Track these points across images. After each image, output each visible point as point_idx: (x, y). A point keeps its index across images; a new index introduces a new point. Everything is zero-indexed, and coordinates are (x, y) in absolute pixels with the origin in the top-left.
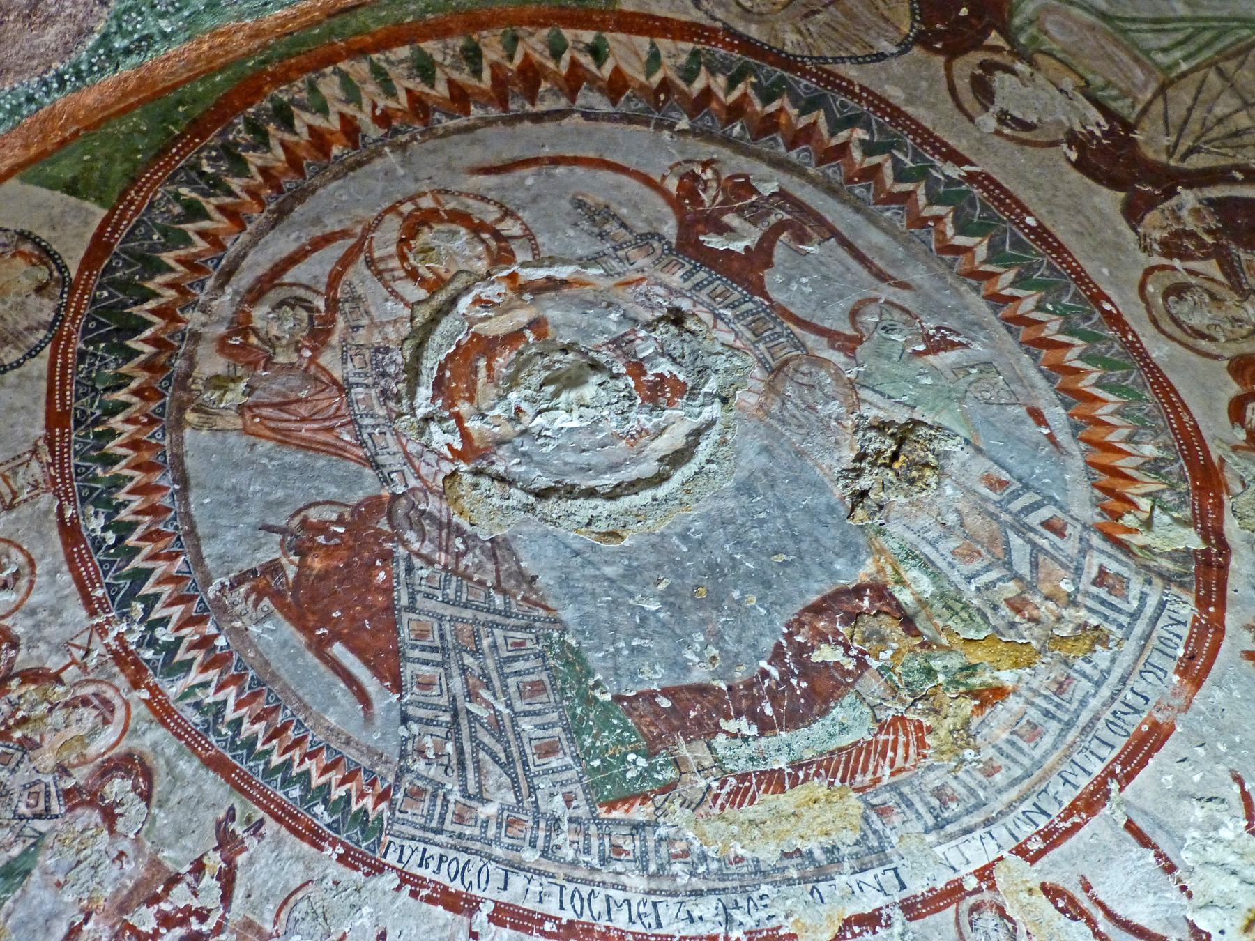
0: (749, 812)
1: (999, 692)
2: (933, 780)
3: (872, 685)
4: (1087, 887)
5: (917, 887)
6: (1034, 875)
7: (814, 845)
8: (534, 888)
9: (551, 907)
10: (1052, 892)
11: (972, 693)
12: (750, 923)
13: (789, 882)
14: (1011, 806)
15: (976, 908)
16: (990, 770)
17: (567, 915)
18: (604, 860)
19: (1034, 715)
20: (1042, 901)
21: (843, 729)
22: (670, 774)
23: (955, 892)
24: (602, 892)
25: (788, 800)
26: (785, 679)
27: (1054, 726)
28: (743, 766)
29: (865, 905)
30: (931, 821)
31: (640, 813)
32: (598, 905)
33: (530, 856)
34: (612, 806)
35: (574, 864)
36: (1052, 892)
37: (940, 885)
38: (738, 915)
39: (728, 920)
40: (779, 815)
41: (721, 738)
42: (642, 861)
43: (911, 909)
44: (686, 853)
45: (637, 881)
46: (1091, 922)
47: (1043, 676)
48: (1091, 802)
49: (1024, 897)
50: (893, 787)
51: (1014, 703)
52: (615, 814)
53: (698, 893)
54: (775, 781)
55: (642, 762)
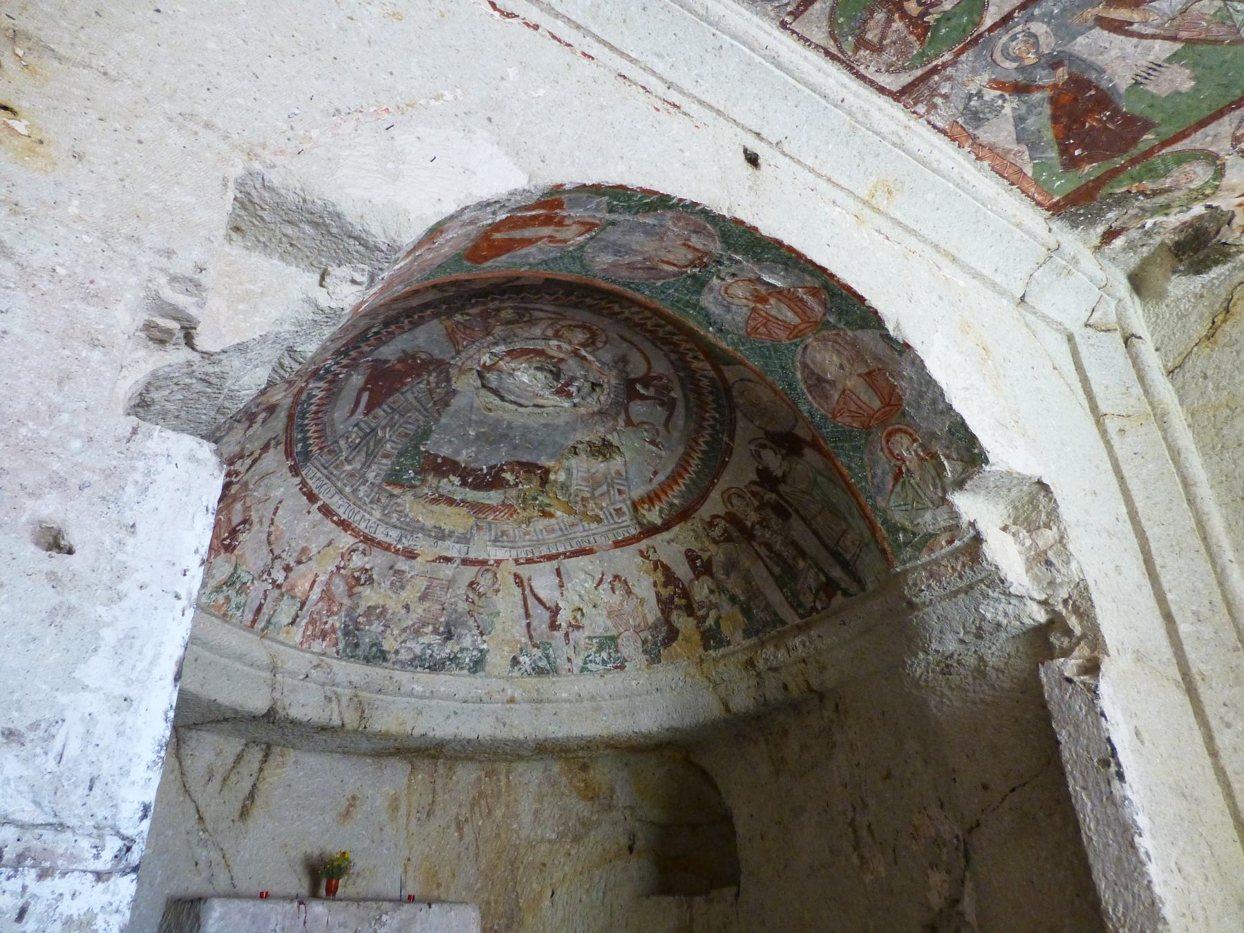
0: (435, 508)
1: (551, 515)
2: (505, 527)
3: (513, 492)
4: (530, 579)
5: (472, 556)
7: (447, 528)
10: (516, 576)
11: (543, 512)
12: (407, 544)
13: (430, 536)
14: (524, 546)
15: (487, 570)
16: (527, 533)
19: (556, 527)
20: (511, 578)
21: (489, 498)
22: (418, 483)
23: (484, 563)
25: (449, 510)
26: (486, 475)
27: (560, 533)
28: (444, 492)
29: (449, 554)
30: (493, 538)
36: (516, 576)
37: (480, 558)
38: (404, 540)
39: (400, 540)
40: (443, 513)
41: (445, 480)
42: (384, 508)
44: (401, 512)
46: (524, 590)
47: (568, 519)
48: (550, 558)
49: (506, 574)
50: (490, 524)
51: (553, 521)
53: (395, 527)
54: (451, 502)
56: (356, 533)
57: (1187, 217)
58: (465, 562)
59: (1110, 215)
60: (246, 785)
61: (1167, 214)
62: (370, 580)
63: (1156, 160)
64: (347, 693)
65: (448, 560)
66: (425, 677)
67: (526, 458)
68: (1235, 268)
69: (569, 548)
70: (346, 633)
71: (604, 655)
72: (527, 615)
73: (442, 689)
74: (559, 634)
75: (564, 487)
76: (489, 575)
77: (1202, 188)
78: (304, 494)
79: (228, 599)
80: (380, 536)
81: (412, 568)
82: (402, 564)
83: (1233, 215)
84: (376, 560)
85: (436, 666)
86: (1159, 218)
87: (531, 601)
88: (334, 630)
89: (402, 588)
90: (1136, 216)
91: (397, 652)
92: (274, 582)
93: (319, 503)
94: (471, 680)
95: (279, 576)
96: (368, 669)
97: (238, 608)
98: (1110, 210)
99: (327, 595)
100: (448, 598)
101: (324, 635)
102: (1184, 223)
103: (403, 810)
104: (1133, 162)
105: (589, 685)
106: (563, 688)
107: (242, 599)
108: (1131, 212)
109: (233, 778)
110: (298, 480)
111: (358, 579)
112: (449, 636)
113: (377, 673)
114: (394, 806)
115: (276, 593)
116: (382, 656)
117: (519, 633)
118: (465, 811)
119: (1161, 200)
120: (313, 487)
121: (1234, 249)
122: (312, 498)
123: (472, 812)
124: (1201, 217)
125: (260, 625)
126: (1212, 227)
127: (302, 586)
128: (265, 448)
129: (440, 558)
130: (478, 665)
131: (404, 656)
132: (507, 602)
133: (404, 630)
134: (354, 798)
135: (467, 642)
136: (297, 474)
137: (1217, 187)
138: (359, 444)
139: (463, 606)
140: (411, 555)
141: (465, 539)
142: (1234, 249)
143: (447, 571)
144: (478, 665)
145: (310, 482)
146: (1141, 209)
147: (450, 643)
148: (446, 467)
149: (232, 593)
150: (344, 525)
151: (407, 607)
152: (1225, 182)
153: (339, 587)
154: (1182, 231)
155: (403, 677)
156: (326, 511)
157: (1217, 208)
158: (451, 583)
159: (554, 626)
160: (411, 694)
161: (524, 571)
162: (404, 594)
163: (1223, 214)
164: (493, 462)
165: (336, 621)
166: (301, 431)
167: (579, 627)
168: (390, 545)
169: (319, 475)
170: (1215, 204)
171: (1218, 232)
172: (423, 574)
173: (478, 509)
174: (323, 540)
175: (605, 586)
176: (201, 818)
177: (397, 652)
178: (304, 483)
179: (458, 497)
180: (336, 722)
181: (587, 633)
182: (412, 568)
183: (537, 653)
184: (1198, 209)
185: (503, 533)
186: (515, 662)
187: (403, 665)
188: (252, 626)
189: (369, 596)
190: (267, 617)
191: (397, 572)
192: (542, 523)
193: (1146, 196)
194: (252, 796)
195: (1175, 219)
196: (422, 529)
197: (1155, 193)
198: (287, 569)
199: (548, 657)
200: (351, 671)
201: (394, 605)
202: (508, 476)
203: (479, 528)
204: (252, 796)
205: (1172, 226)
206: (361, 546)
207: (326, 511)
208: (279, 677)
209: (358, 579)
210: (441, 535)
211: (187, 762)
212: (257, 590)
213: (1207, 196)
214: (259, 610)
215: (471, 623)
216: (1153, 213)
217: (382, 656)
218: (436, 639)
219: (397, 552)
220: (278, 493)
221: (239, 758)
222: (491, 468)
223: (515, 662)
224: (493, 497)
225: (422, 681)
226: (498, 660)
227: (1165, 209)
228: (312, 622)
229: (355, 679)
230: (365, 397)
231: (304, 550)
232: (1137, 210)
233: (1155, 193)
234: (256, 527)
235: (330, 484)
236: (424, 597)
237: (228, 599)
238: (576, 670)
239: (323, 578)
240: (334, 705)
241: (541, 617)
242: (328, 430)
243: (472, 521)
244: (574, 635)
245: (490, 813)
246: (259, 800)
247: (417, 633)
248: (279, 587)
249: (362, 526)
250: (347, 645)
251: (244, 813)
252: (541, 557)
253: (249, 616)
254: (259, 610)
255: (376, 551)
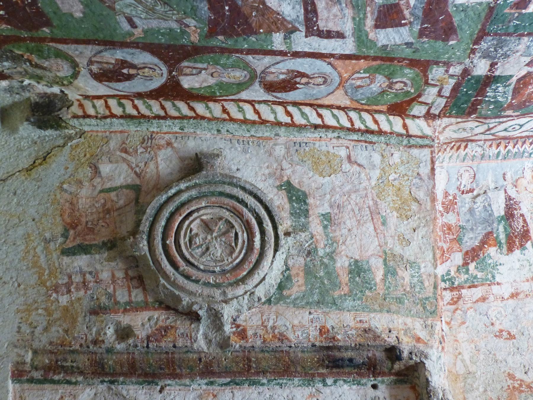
57: (49, 90)
59: (5, 64)
61: (38, 83)
63: (45, 46)
68: (60, 135)
77: (62, 78)
83: (72, 105)
86: (33, 82)
90: (20, 73)
98: (7, 60)
102: (46, 94)
104: (32, 39)
108: (19, 69)
119: (39, 72)
121: (64, 124)
124: (55, 95)
126: (59, 104)
137: (71, 83)
142: (64, 124)
146: (26, 71)
152: (76, 82)
154: (42, 97)
157: (66, 95)
163: (68, 100)
170: (66, 92)
171: (60, 109)
184: (56, 90)
193: (31, 64)
195: (41, 88)
197: (37, 66)
205: (38, 91)
213: (63, 85)
216: (32, 77)
227: (39, 79)
232: (22, 70)
233: (37, 66)
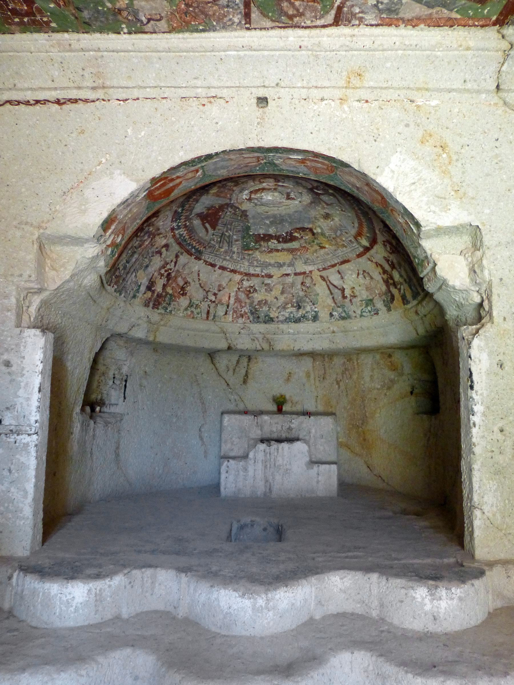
2: (307, 256)
4: (327, 277)
5: (298, 271)
6: (319, 273)
7: (281, 262)
8: (227, 263)
9: (230, 266)
14: (319, 263)
15: (307, 276)
17: (232, 268)
18: (241, 259)
20: (319, 277)
22: (258, 247)
23: (304, 273)
24: (240, 265)
25: (278, 254)
28: (273, 247)
30: (304, 262)
31: (250, 252)
32: (238, 267)
33: (228, 258)
34: (245, 250)
35: (236, 259)
37: (302, 271)
40: (276, 256)
41: (270, 243)
42: (248, 260)
43: (296, 274)
44: (257, 260)
45: (247, 263)
49: (316, 276)
50: (299, 256)
52: (246, 252)
54: (277, 251)
55: (254, 244)
56: (240, 273)
58: (296, 274)
60: (243, 371)
62: (255, 290)
64: (260, 337)
65: (288, 275)
66: (293, 325)
67: (299, 226)
69: (339, 261)
70: (252, 313)
71: (369, 308)
72: (331, 294)
73: (302, 330)
74: (347, 300)
75: (323, 234)
76: (309, 278)
78: (208, 265)
79: (192, 312)
80: (252, 271)
81: (272, 282)
82: (267, 281)
84: (255, 282)
85: (297, 321)
87: (331, 287)
88: (246, 313)
89: (271, 290)
91: (277, 317)
92: (211, 301)
93: (218, 267)
94: (314, 324)
95: (213, 298)
96: (267, 326)
97: (198, 314)
99: (238, 300)
100: (293, 291)
101: (242, 316)
103: (312, 377)
105: (365, 322)
106: (355, 324)
107: (199, 310)
109: (237, 369)
110: (202, 261)
111: (250, 291)
112: (299, 307)
113: (271, 327)
114: (308, 375)
115: (214, 304)
116: (271, 320)
117: (330, 301)
118: (340, 377)
120: (211, 261)
122: (213, 265)
123: (343, 377)
125: (211, 317)
127: (225, 299)
128: (177, 256)
129: (283, 275)
130: (315, 318)
131: (281, 318)
132: (321, 288)
133: (278, 308)
134: (290, 373)
135: (308, 308)
136: (200, 259)
138: (221, 240)
139: (302, 294)
140: (270, 276)
141: (291, 264)
143: (289, 280)
144: (315, 318)
145: (208, 260)
147: (301, 310)
148: (267, 238)
149: (192, 309)
150: (234, 271)
151: (276, 298)
153: (242, 296)
155: (284, 327)
156: (223, 268)
158: (293, 285)
159: (344, 297)
160: (289, 333)
161: (324, 273)
162: (273, 293)
164: (286, 231)
165: (246, 309)
166: (189, 246)
167: (355, 297)
168: (258, 274)
169: (211, 256)
172: (279, 283)
173: (291, 251)
174: (227, 280)
175: (361, 276)
176: (228, 385)
177: (277, 317)
178: (205, 261)
179: (280, 248)
180: (259, 348)
181: (359, 299)
182: (272, 282)
183: (340, 310)
185: (308, 259)
186: (331, 315)
187: (282, 322)
188: (207, 318)
189: (257, 297)
190: (213, 314)
191: (266, 285)
192: (322, 251)
194: (246, 375)
196: (270, 264)
198: (215, 294)
199: (345, 311)
200: (258, 328)
201: (270, 298)
202: (296, 234)
203: (296, 259)
204: (246, 375)
206: (245, 278)
207: (223, 268)
208: (228, 335)
209: (250, 291)
210: (280, 266)
211: (218, 365)
212: (204, 306)
214: (208, 312)
215: (307, 300)
217: (271, 320)
218: (294, 310)
219: (263, 276)
220: (197, 268)
221: (238, 362)
222: (287, 233)
223: (331, 315)
224: (295, 245)
225: (292, 327)
226: (324, 315)
228: (235, 312)
229: (262, 331)
230: (207, 225)
231: (220, 286)
234: (192, 283)
235: (218, 258)
236: (282, 293)
237: (192, 312)
238: (358, 316)
239: (233, 294)
240: (256, 341)
241: (337, 293)
242: (202, 241)
243: (291, 256)
244: (354, 300)
245: (351, 377)
246: (250, 376)
247: (285, 308)
248: (214, 302)
249: (242, 270)
250: (254, 318)
251: (245, 382)
252: (329, 266)
253: (204, 316)
254: (208, 312)
255: (253, 278)
